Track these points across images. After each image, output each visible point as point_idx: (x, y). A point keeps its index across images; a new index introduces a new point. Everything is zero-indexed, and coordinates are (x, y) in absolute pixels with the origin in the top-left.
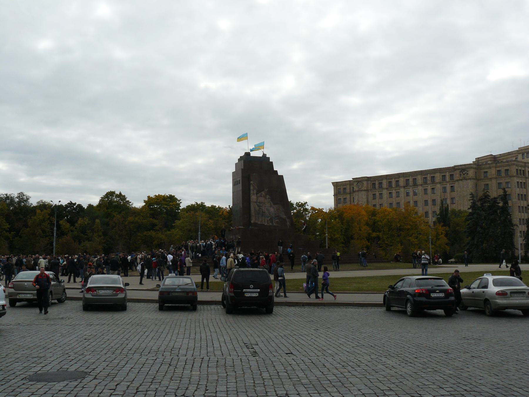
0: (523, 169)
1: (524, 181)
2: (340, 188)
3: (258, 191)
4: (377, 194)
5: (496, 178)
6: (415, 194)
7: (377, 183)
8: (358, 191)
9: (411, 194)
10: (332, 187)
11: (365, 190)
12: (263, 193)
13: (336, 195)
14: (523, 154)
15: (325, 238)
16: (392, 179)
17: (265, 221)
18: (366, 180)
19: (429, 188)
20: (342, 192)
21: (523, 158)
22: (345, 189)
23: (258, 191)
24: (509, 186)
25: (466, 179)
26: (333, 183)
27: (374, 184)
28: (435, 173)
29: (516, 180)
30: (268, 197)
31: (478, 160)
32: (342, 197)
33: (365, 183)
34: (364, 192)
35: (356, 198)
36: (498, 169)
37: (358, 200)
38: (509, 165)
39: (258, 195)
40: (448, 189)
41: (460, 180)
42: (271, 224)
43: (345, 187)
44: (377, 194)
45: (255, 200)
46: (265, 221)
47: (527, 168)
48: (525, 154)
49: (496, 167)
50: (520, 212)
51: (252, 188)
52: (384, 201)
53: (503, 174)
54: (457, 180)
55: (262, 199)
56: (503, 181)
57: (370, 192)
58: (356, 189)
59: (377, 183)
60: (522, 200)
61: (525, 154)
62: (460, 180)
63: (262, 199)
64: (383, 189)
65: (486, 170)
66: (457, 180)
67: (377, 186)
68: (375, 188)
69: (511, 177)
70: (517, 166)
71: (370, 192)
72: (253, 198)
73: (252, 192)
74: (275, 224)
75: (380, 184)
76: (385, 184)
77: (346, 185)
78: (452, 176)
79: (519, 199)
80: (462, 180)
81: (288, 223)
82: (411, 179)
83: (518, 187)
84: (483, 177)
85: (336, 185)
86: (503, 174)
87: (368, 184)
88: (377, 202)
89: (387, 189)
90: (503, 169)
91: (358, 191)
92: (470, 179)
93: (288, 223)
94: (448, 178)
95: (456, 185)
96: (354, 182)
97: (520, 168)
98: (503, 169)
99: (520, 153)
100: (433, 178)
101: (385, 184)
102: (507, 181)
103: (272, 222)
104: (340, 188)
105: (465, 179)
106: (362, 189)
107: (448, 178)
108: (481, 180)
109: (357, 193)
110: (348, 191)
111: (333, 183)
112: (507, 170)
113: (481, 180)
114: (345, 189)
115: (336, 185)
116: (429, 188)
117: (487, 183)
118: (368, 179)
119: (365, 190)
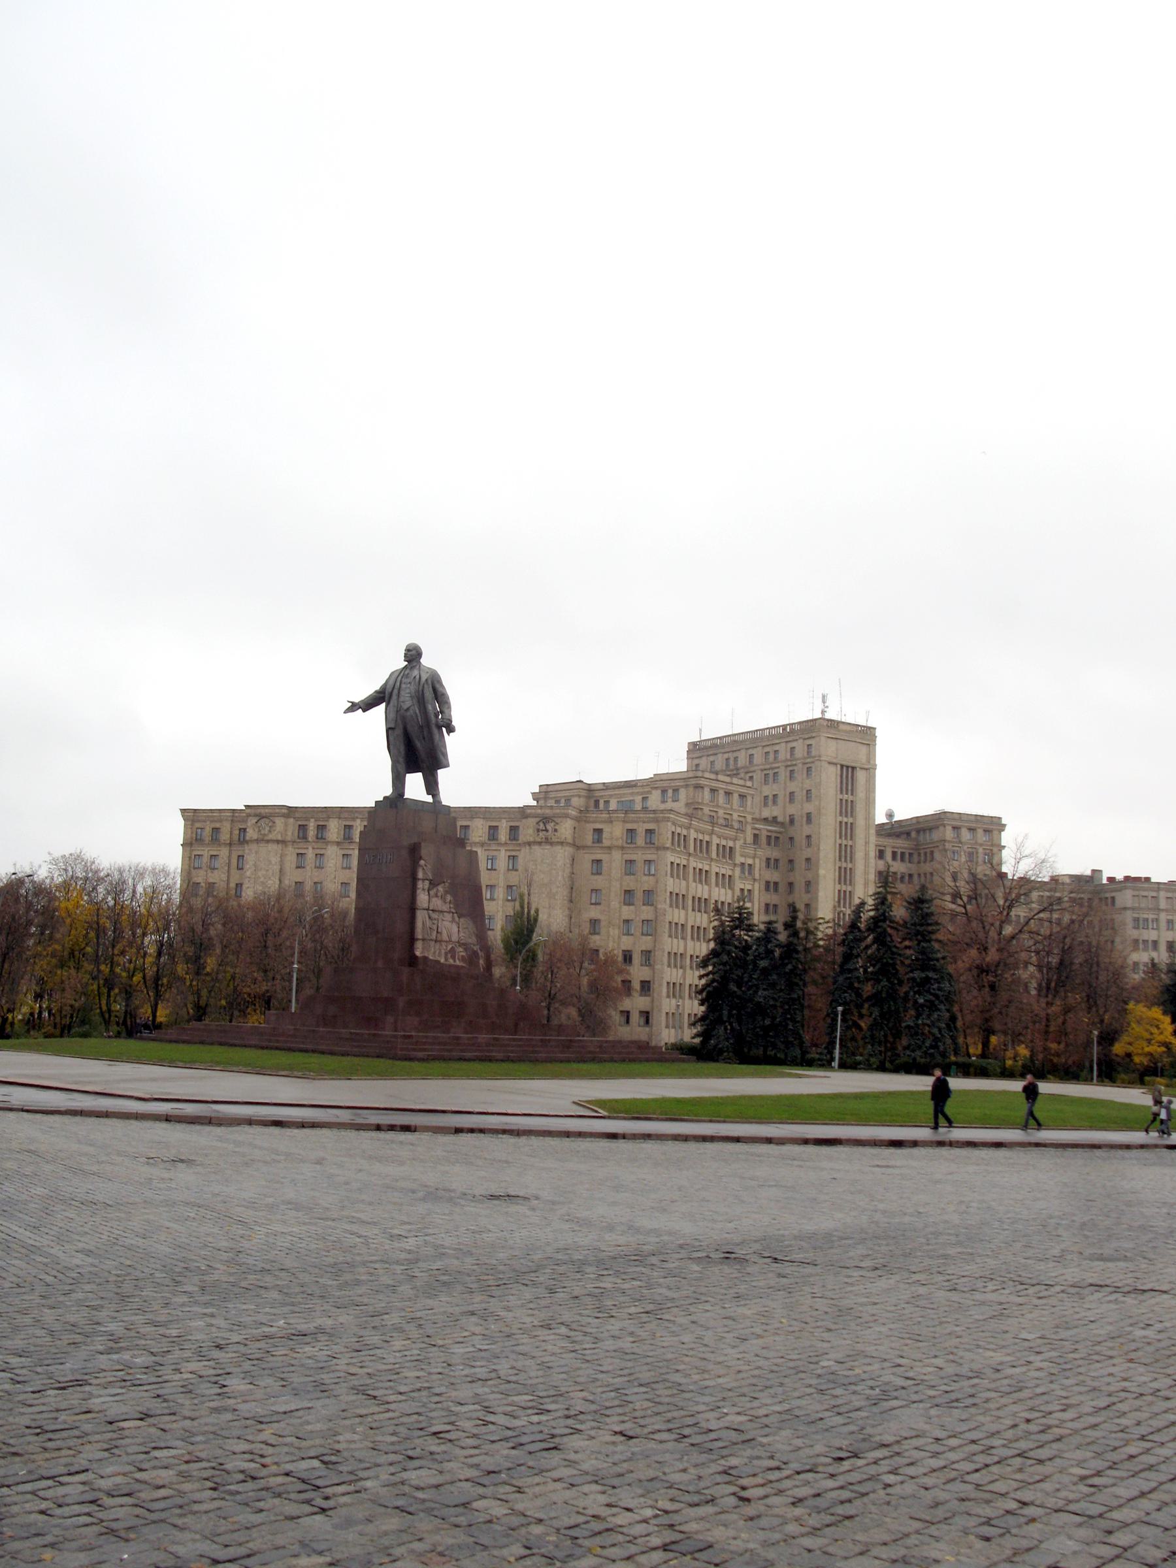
0: (684, 832)
1: (684, 862)
3: (433, 884)
4: (310, 854)
5: (622, 848)
8: (257, 841)
11: (278, 842)
12: (440, 888)
13: (188, 844)
14: (664, 792)
15: (290, 974)
16: (354, 819)
17: (440, 955)
18: (286, 816)
20: (207, 839)
21: (663, 802)
22: (216, 830)
23: (433, 884)
24: (653, 872)
25: (552, 844)
26: (183, 811)
28: (472, 818)
29: (670, 857)
30: (449, 898)
31: (545, 793)
32: (206, 852)
33: (279, 822)
34: (272, 847)
35: (250, 860)
36: (630, 826)
37: (255, 865)
38: (657, 821)
39: (432, 893)
41: (535, 843)
42: (451, 961)
43: (218, 825)
44: (310, 854)
45: (426, 906)
46: (440, 955)
47: (692, 831)
48: (670, 792)
49: (624, 821)
50: (670, 936)
51: (420, 875)
53: (640, 840)
54: (529, 844)
55: (437, 903)
56: (639, 857)
57: (290, 848)
58: (251, 834)
60: (677, 907)
61: (670, 792)
62: (535, 843)
63: (437, 903)
64: (327, 843)
65: (598, 826)
66: (529, 844)
67: (312, 833)
68: (305, 838)
69: (658, 849)
70: (674, 824)
71: (290, 848)
72: (422, 898)
73: (420, 885)
74: (458, 963)
75: (321, 828)
76: (334, 829)
77: (221, 821)
78: (514, 830)
79: (671, 906)
80: (540, 843)
81: (481, 962)
83: (672, 876)
84: (589, 843)
85: (192, 817)
86: (640, 840)
87: (286, 825)
88: (309, 876)
89: (338, 843)
90: (641, 829)
91: (257, 841)
92: (562, 843)
93: (481, 962)
94: (503, 836)
95: (523, 855)
96: (249, 815)
97: (679, 830)
98: (641, 829)
99: (656, 788)
101: (334, 829)
102: (649, 857)
103: (453, 957)
104: (205, 830)
105: (548, 841)
106: (271, 837)
107: (503, 836)
108: (584, 847)
109: (254, 847)
110: (225, 836)
111: (183, 811)
112: (650, 832)
113: (584, 847)
114: (216, 830)
115: (192, 817)
117: (598, 857)
119: (278, 842)
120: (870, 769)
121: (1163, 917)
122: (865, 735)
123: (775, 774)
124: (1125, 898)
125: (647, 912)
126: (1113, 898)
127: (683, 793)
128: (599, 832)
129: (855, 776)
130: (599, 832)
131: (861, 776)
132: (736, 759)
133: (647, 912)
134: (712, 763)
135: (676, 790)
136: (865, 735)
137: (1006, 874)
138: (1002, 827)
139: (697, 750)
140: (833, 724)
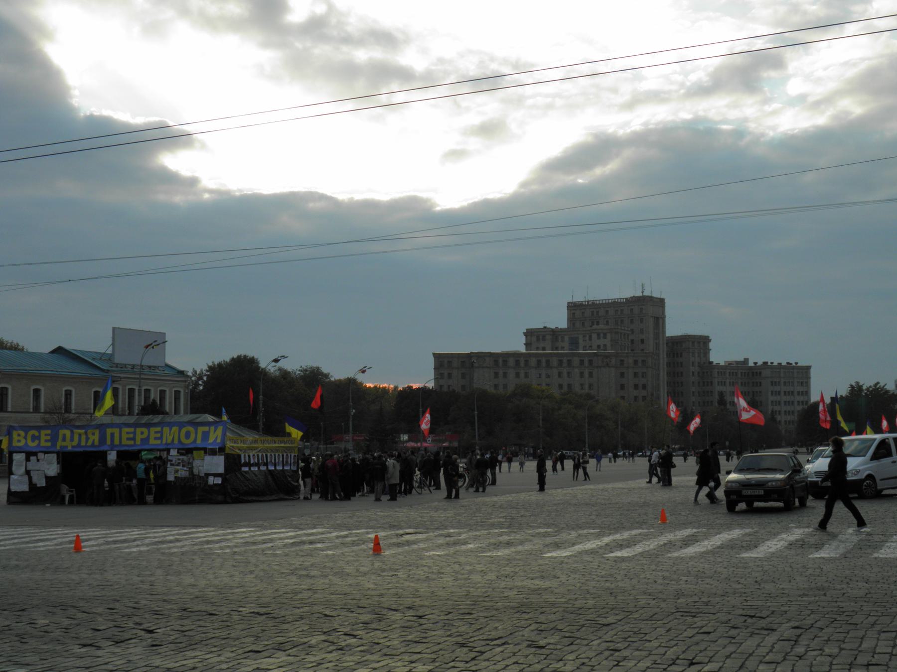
2: (443, 362)
4: (501, 373)
6: (548, 376)
7: (501, 361)
9: (544, 376)
10: (432, 360)
14: (598, 335)
19: (565, 371)
22: (450, 362)
26: (434, 354)
27: (496, 362)
40: (586, 375)
44: (501, 373)
48: (602, 335)
52: (483, 381)
53: (640, 364)
54: (597, 367)
59: (501, 361)
61: (602, 335)
66: (597, 367)
75: (505, 362)
76: (511, 362)
78: (591, 362)
82: (544, 360)
85: (438, 357)
94: (586, 363)
100: (569, 362)
101: (511, 362)
104: (443, 362)
107: (586, 363)
111: (434, 354)
115: (438, 357)
116: (565, 371)
118: (491, 355)
120: (663, 318)
121: (783, 380)
122: (661, 302)
123: (622, 321)
124: (766, 373)
125: (644, 393)
126: (760, 373)
127: (609, 336)
128: (622, 361)
129: (659, 321)
130: (622, 361)
131: (661, 321)
132: (598, 312)
133: (644, 393)
134: (583, 313)
135: (605, 335)
136: (661, 302)
137: (712, 363)
138: (710, 341)
139: (573, 307)
140: (651, 298)
